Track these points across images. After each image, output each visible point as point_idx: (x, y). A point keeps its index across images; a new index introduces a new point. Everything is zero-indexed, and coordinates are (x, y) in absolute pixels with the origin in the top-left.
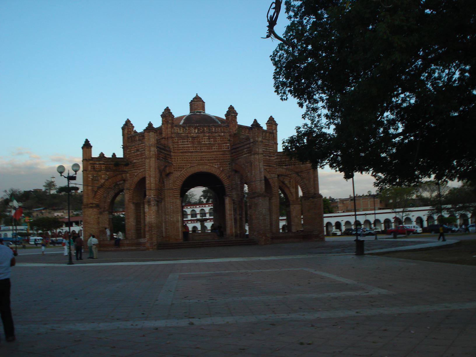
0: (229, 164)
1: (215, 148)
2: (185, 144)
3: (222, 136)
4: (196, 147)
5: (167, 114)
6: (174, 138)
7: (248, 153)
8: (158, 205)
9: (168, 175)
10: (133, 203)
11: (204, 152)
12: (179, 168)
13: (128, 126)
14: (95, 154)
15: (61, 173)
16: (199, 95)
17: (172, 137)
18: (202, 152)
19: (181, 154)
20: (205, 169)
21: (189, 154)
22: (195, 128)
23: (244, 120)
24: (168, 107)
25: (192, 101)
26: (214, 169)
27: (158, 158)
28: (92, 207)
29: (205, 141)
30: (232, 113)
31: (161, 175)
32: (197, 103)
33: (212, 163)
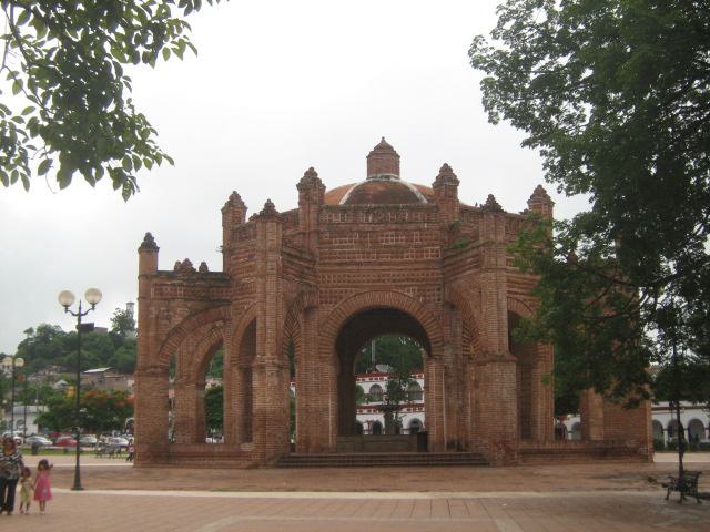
0: (439, 290)
4: (369, 253)
5: (310, 184)
7: (476, 267)
8: (279, 375)
9: (308, 311)
10: (240, 368)
12: (331, 297)
13: (234, 207)
14: (166, 263)
15: (66, 306)
16: (389, 141)
17: (318, 232)
18: (381, 264)
19: (337, 268)
20: (387, 299)
21: (354, 267)
22: (368, 213)
23: (470, 195)
24: (312, 169)
25: (372, 154)
26: (405, 299)
27: (282, 272)
28: (153, 374)
29: (387, 241)
30: (447, 180)
31: (289, 311)
32: (383, 158)
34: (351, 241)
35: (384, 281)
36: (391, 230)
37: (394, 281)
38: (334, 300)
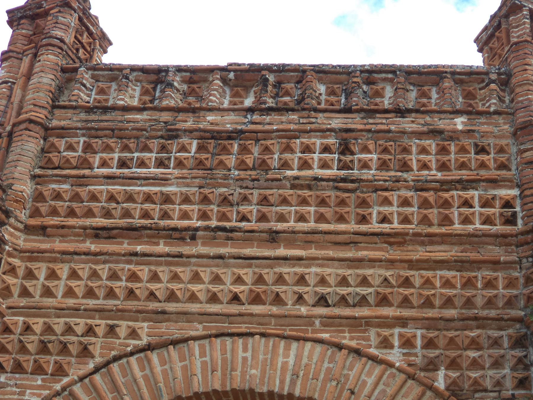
1: (390, 213)
2: (133, 179)
3: (454, 135)
6: (63, 132)
11: (292, 238)
18: (274, 237)
33: (357, 324)
34: (160, 164)
35: (278, 300)
36: (324, 132)
37: (322, 301)
38: (50, 362)
